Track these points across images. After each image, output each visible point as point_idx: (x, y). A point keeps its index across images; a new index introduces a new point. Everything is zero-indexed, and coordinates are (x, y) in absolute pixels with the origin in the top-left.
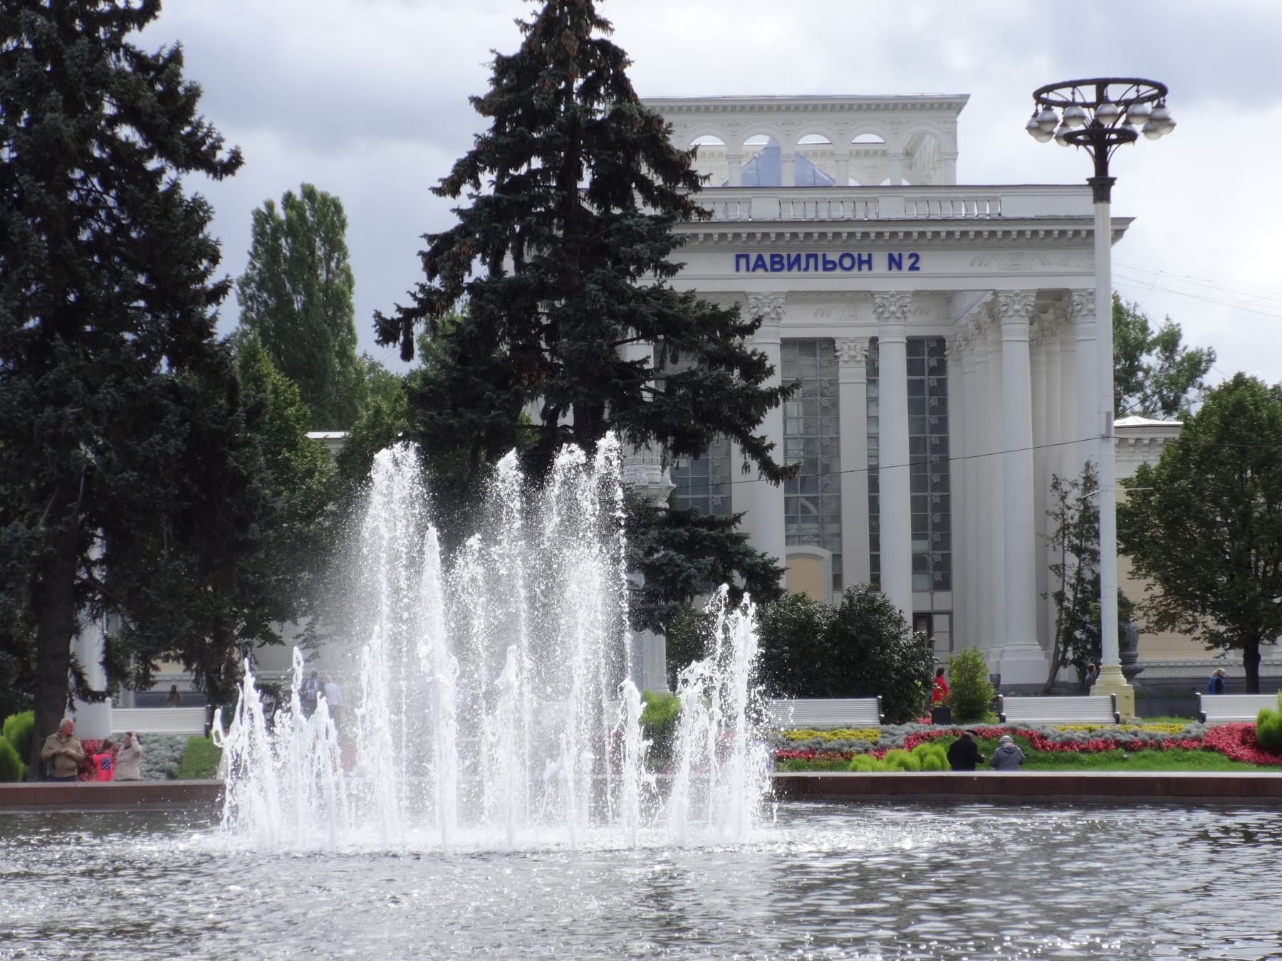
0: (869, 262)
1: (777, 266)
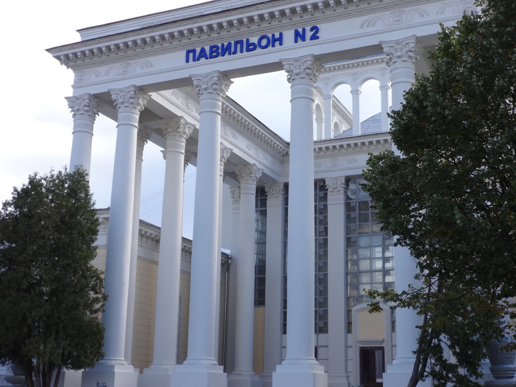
0: (280, 40)
1: (214, 54)
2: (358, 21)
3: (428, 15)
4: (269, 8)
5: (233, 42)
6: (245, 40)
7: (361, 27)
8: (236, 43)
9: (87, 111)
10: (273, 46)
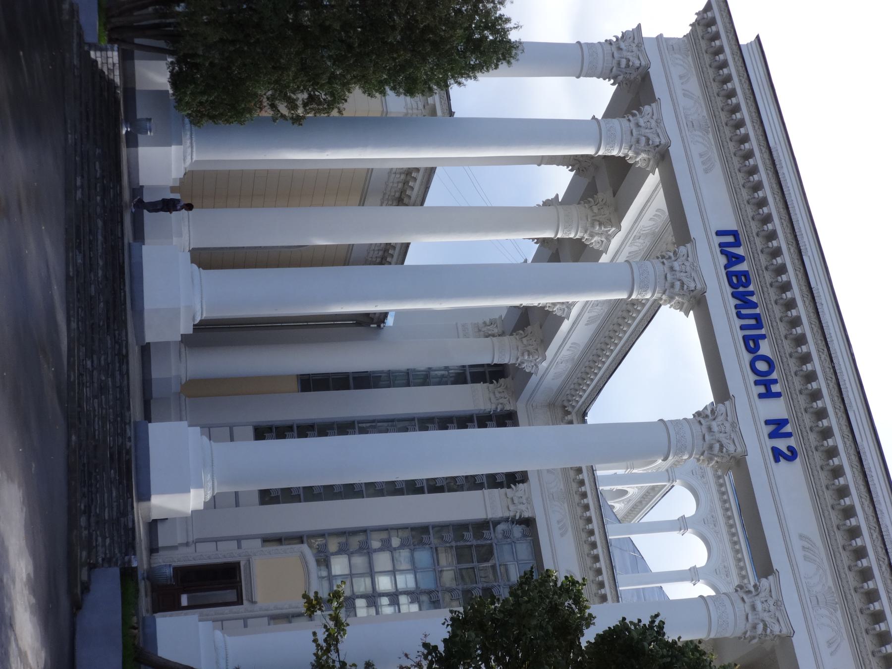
0: (768, 394)
1: (735, 280)
2: (812, 529)
3: (832, 654)
4: (824, 372)
5: (757, 311)
6: (763, 331)
7: (801, 537)
8: (757, 317)
9: (619, 64)
10: (757, 383)
